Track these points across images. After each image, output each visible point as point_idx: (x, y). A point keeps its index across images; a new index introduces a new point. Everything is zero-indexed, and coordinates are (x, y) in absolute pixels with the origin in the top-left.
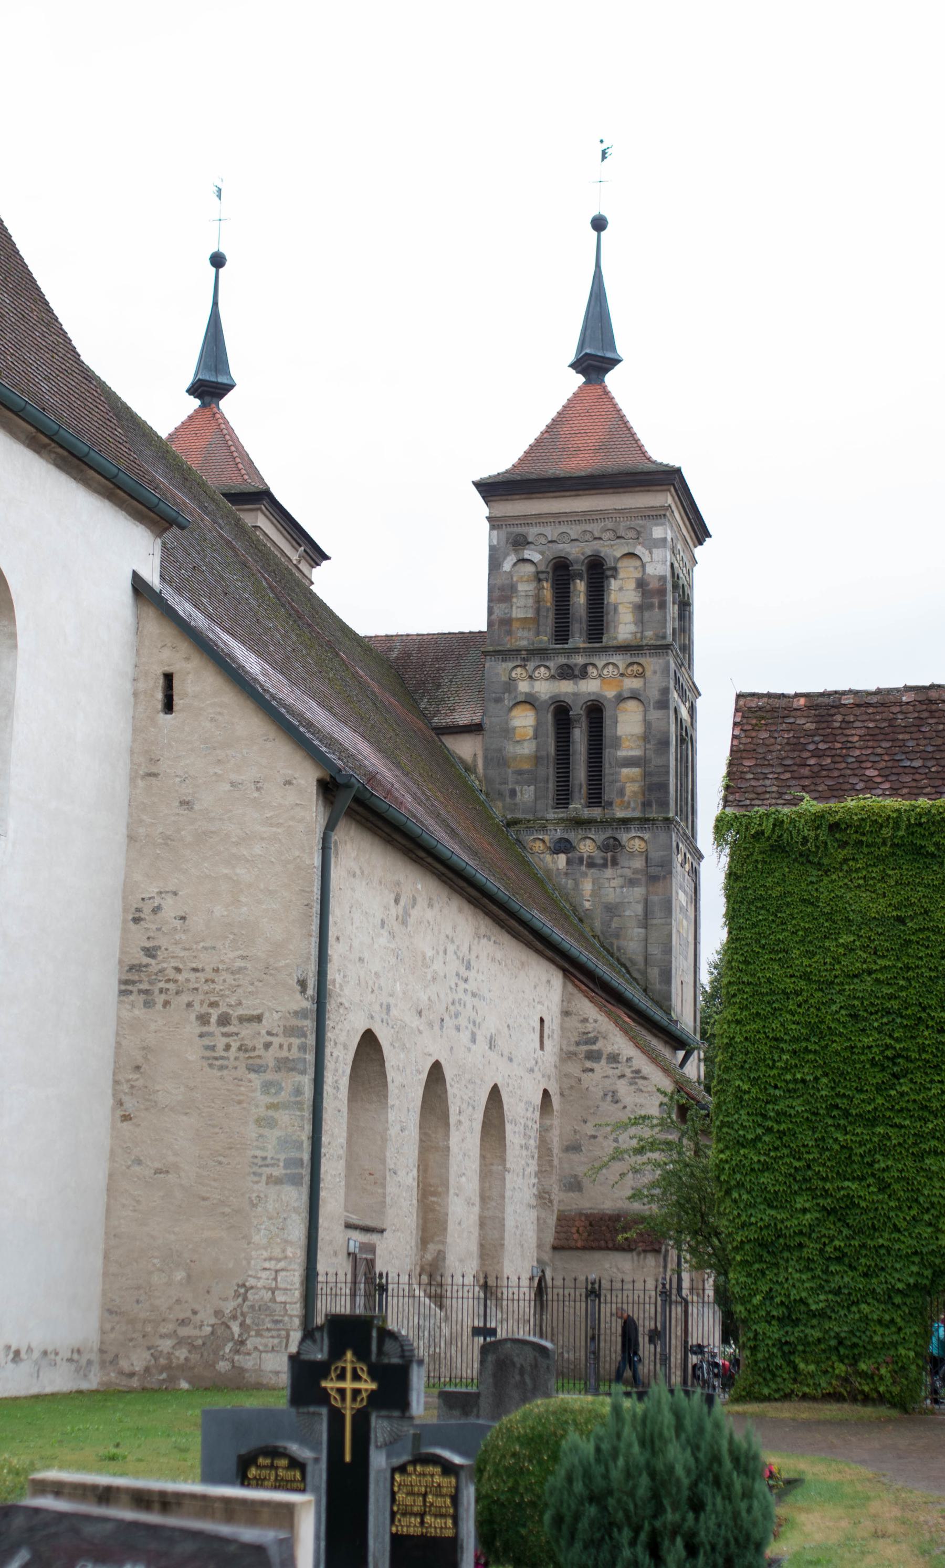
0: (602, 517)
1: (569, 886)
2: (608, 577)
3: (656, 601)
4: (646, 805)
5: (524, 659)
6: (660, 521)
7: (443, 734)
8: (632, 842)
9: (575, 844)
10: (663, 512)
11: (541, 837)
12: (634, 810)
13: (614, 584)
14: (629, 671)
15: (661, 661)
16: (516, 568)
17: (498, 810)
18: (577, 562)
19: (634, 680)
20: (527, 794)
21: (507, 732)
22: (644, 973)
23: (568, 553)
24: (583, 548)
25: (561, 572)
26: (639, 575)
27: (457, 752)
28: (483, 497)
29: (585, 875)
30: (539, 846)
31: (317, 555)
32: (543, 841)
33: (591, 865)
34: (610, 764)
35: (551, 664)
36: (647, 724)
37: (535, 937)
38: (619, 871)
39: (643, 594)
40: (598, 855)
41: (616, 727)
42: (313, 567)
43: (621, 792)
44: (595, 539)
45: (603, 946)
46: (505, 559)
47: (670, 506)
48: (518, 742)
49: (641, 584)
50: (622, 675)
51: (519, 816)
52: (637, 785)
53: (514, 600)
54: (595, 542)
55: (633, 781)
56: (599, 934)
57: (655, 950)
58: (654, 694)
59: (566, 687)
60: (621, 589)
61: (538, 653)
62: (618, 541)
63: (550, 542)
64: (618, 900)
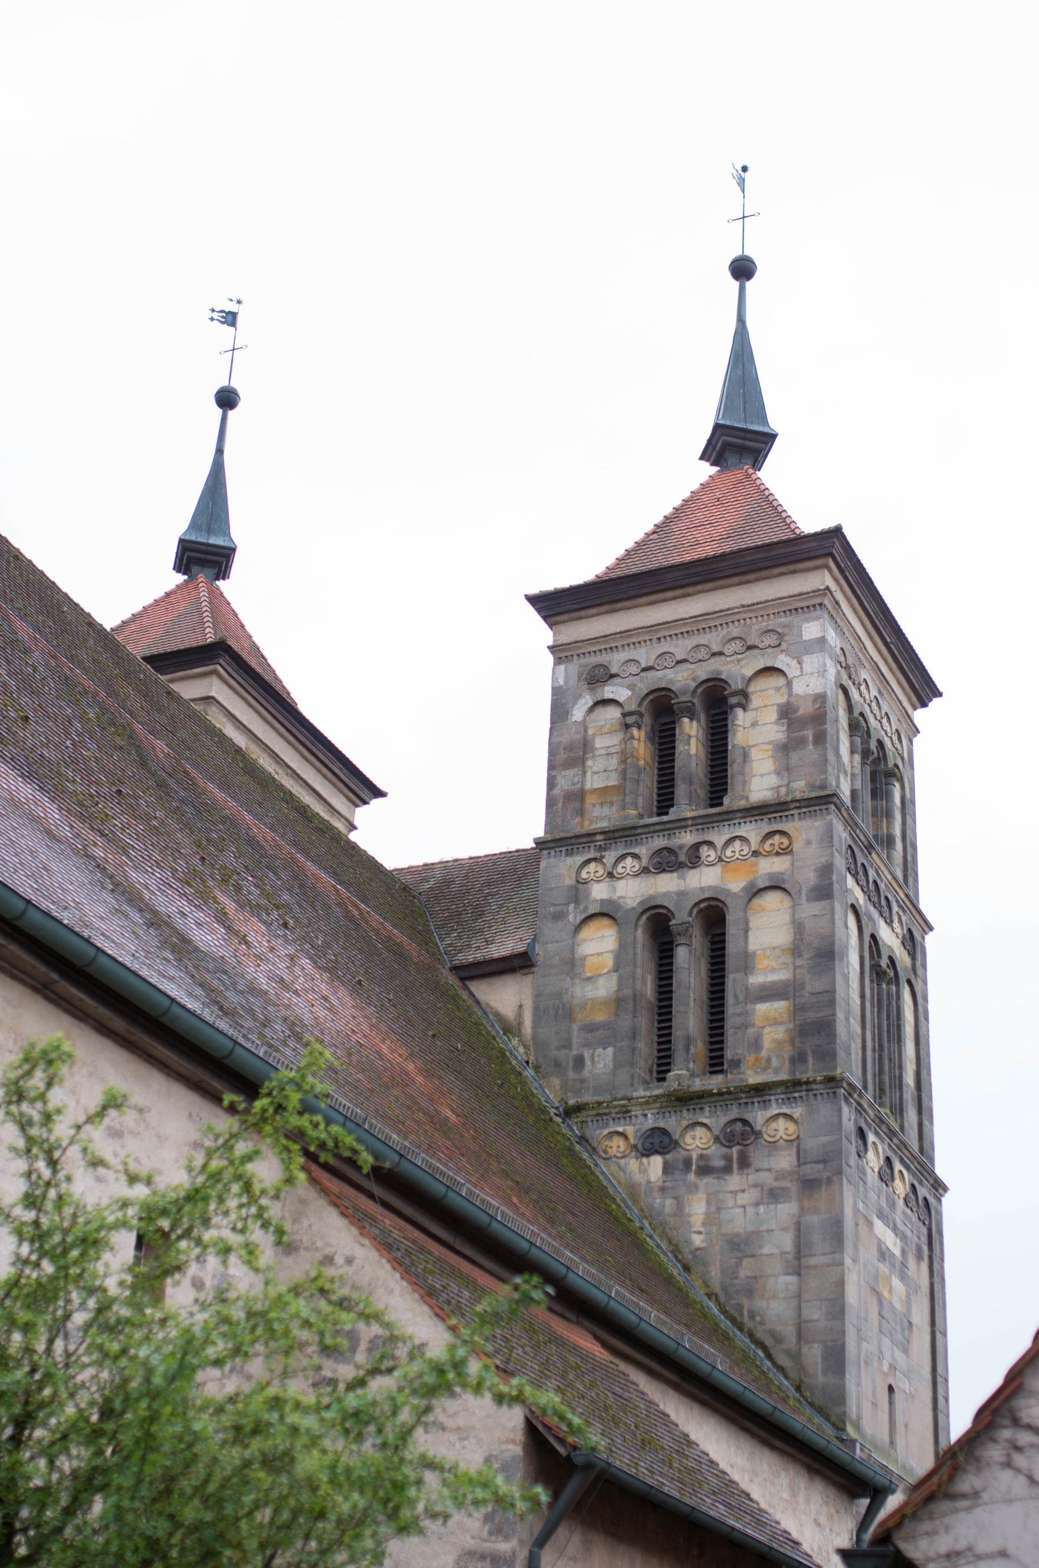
0: (723, 621)
1: (667, 1210)
2: (732, 707)
3: (809, 734)
4: (798, 1059)
5: (600, 849)
6: (814, 614)
7: (472, 978)
8: (774, 1125)
9: (676, 1136)
10: (818, 601)
11: (620, 1129)
12: (777, 1071)
13: (741, 718)
14: (767, 846)
15: (817, 824)
16: (594, 715)
17: (551, 1093)
18: (684, 693)
19: (776, 859)
20: (601, 1062)
21: (572, 965)
22: (796, 1356)
23: (672, 681)
24: (694, 671)
25: (661, 712)
26: (782, 700)
27: (493, 1004)
28: (545, 618)
29: (696, 1187)
30: (618, 1146)
31: (362, 789)
32: (623, 1135)
33: (705, 1170)
34: (736, 997)
35: (643, 851)
36: (798, 927)
37: (62, 973)
38: (752, 1178)
39: (789, 725)
40: (716, 1154)
41: (746, 938)
42: (357, 806)
43: (756, 1044)
44: (714, 654)
45: (724, 1312)
46: (575, 703)
47: (828, 588)
48: (589, 979)
49: (786, 713)
50: (756, 854)
51: (587, 1098)
52: (781, 1029)
53: (589, 763)
54: (713, 660)
55: (776, 1022)
56: (717, 1289)
57: (815, 1313)
58: (808, 877)
59: (665, 885)
60: (754, 724)
61: (622, 835)
62: (748, 653)
63: (645, 670)
64: (749, 1229)
